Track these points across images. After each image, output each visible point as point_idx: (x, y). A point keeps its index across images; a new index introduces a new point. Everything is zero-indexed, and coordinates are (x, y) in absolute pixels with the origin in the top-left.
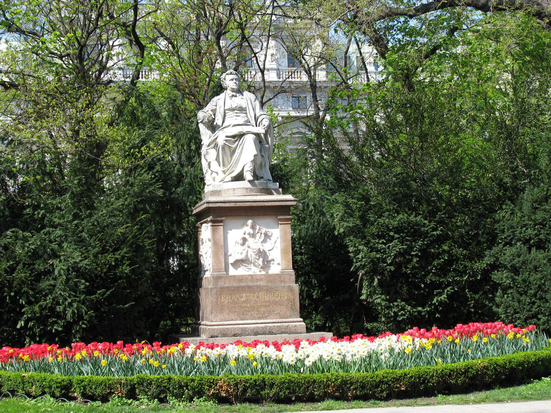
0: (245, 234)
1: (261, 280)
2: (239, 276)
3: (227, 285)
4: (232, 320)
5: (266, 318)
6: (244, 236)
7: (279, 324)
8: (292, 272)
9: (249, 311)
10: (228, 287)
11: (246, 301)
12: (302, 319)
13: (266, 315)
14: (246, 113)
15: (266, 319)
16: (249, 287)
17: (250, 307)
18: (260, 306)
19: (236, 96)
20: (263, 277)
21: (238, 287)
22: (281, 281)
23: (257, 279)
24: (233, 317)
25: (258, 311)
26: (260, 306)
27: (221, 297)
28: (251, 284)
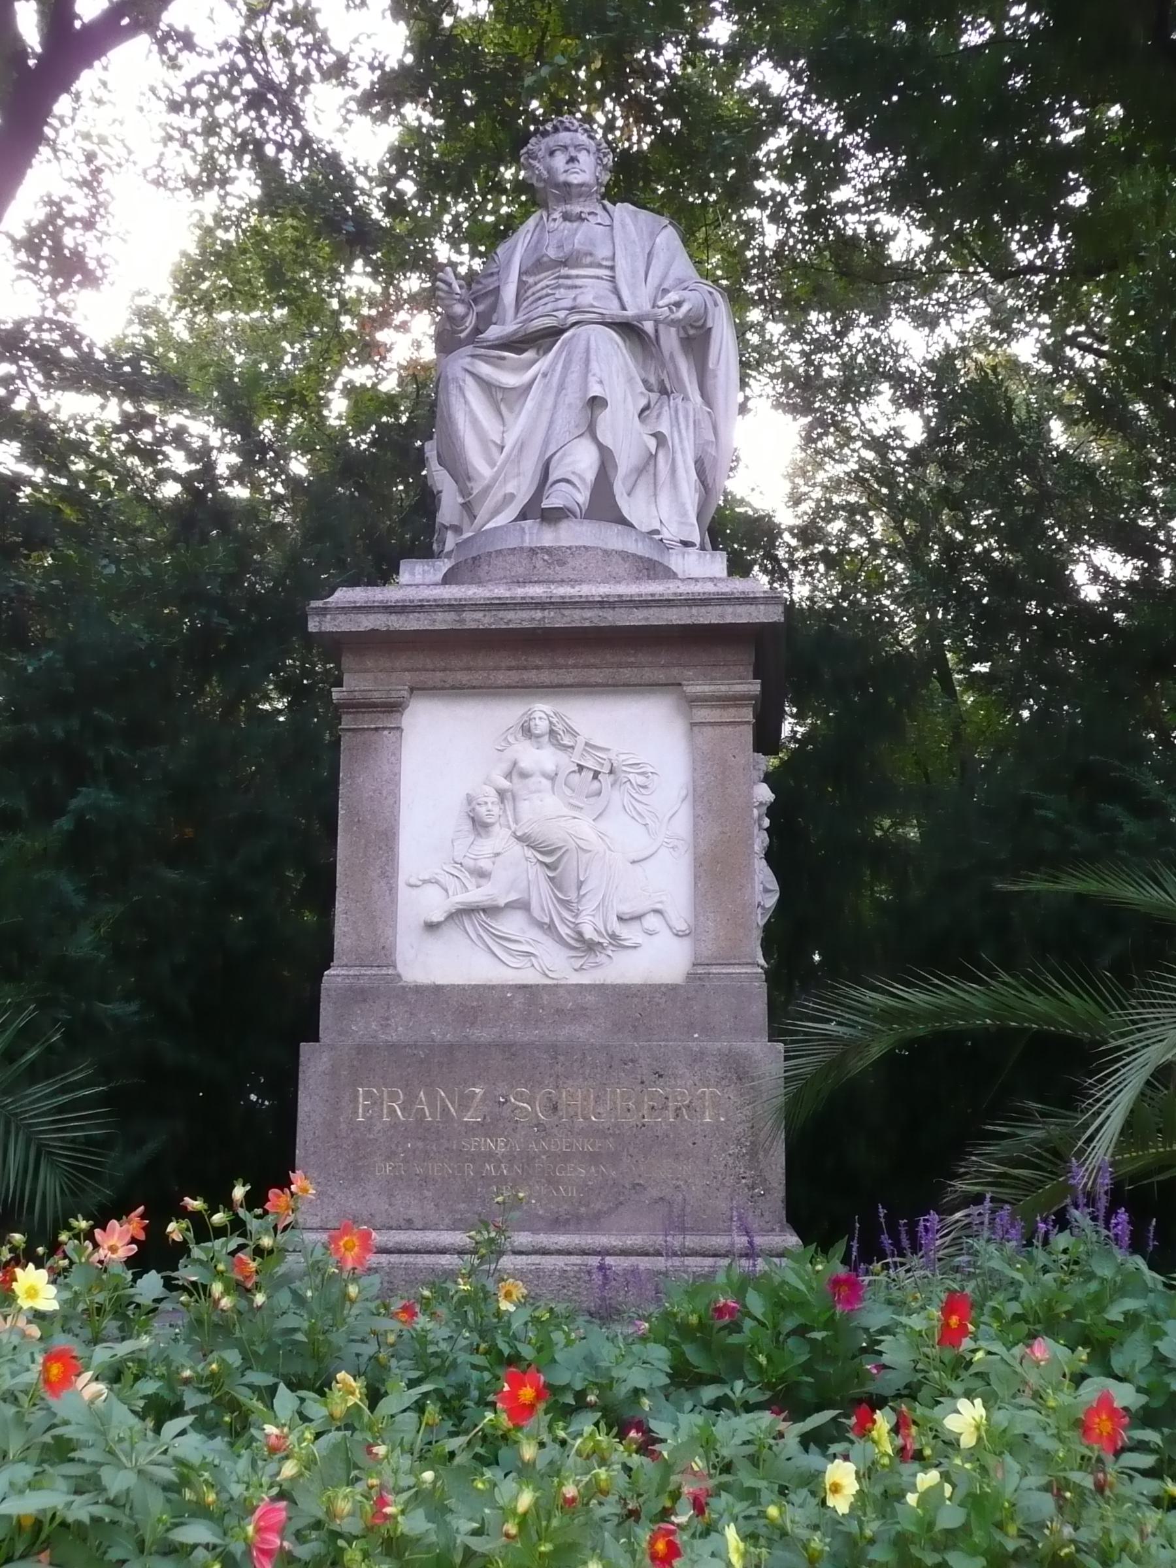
0: (508, 776)
1: (580, 1014)
2: (461, 989)
3: (393, 1037)
4: (409, 1225)
5: (594, 1222)
6: (505, 784)
7: (660, 1263)
8: (752, 977)
9: (502, 1180)
10: (393, 1048)
11: (487, 1128)
12: (792, 1240)
13: (598, 1206)
14: (613, 279)
15: (593, 1230)
16: (509, 1049)
17: (511, 1158)
18: (566, 1157)
19: (580, 218)
20: (590, 999)
21: (451, 1048)
22: (691, 1027)
23: (559, 1011)
24: (414, 1212)
25: (553, 1182)
26: (566, 1157)
27: (354, 1099)
28: (521, 1035)
